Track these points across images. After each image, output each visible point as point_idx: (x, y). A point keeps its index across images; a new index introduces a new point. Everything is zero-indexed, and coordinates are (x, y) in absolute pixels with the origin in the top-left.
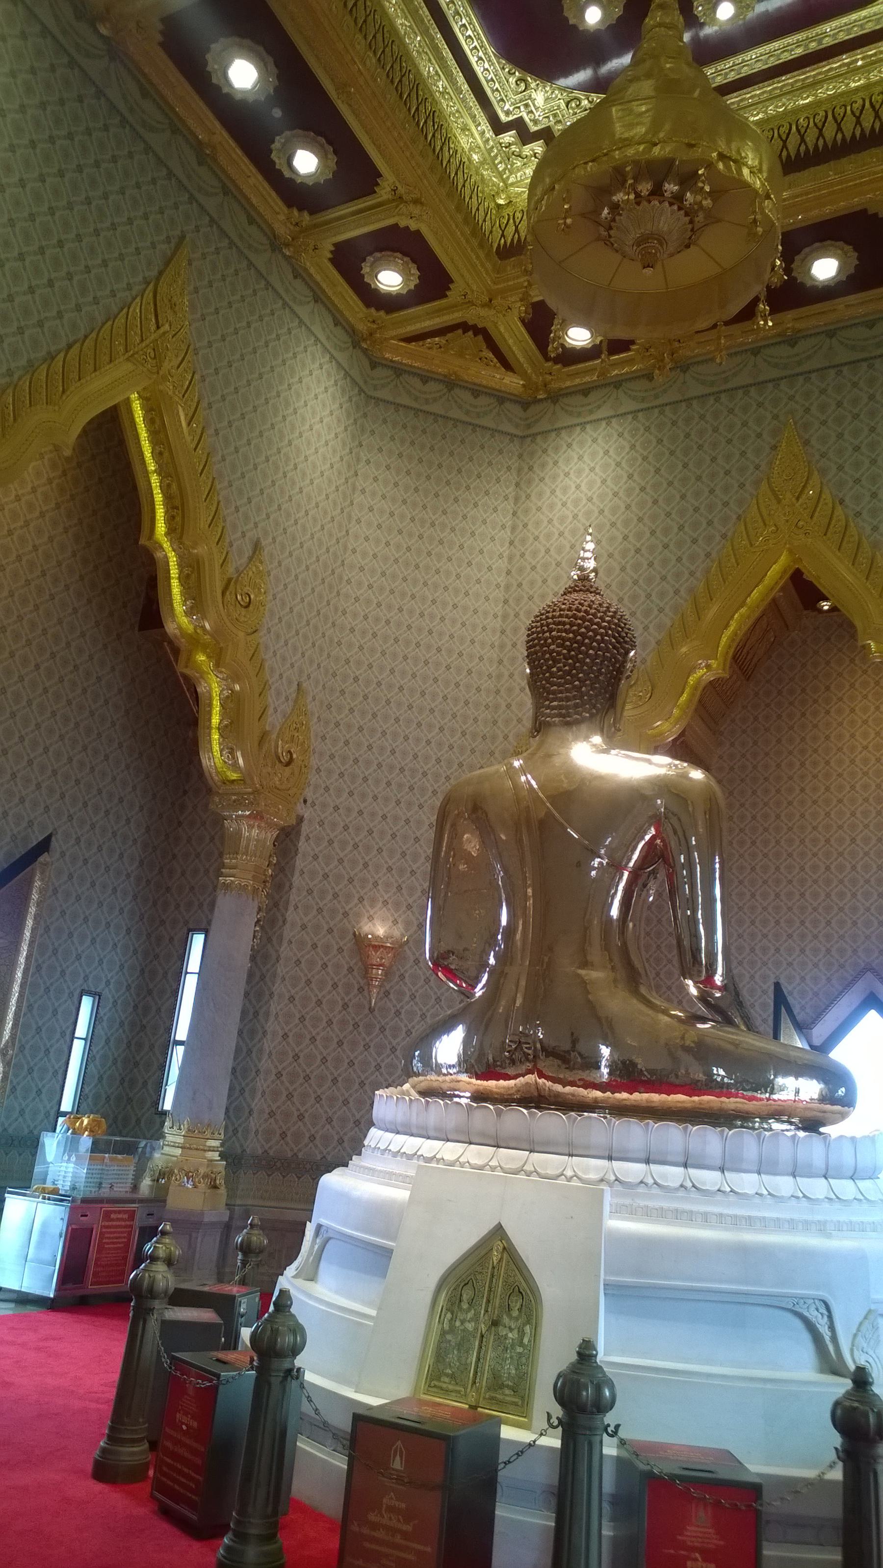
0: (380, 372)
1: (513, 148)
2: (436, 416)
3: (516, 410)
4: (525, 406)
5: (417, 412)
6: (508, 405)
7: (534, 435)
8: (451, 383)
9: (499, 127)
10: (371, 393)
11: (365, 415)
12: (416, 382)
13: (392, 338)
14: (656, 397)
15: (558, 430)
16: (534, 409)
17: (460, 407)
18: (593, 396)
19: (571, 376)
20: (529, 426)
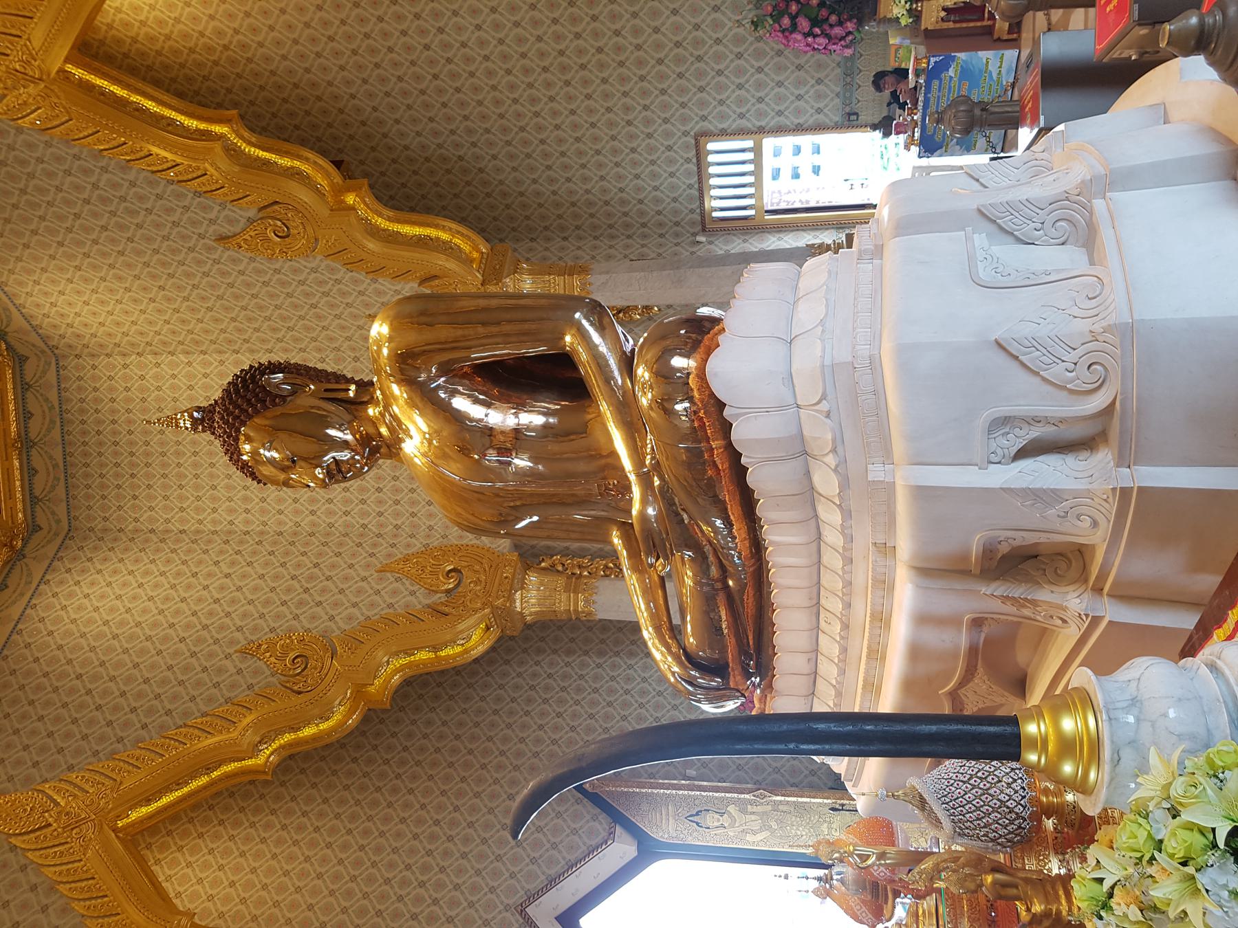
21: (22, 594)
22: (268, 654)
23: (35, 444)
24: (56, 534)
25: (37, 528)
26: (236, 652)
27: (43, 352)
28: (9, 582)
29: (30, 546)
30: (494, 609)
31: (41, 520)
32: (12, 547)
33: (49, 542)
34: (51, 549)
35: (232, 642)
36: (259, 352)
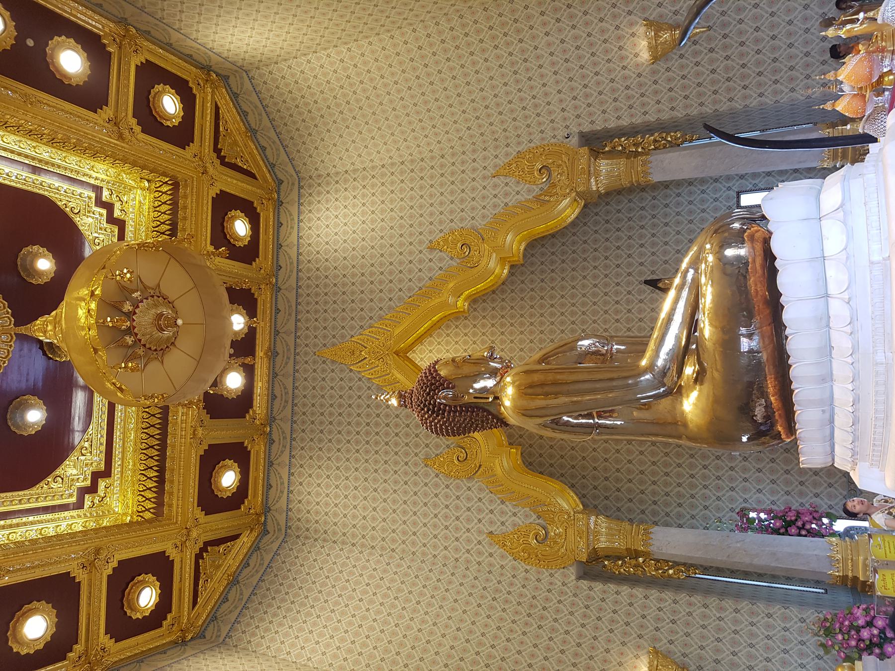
0: (208, 634)
1: (96, 501)
2: (253, 593)
3: (266, 539)
4: (266, 532)
5: (245, 607)
6: (261, 545)
7: (288, 527)
8: (234, 581)
9: (79, 505)
10: (221, 640)
11: (236, 646)
12: (225, 606)
13: (189, 614)
14: (285, 438)
15: (289, 510)
16: (270, 528)
17: (252, 576)
18: (273, 482)
19: (255, 495)
20: (279, 530)
21: (292, 228)
22: (445, 247)
23: (257, 131)
24: (293, 184)
25: (281, 182)
26: (424, 249)
27: (236, 71)
28: (281, 220)
29: (282, 194)
30: (578, 194)
31: (280, 176)
32: (273, 199)
33: (291, 190)
34: (294, 195)
35: (421, 242)
36: (371, 37)
